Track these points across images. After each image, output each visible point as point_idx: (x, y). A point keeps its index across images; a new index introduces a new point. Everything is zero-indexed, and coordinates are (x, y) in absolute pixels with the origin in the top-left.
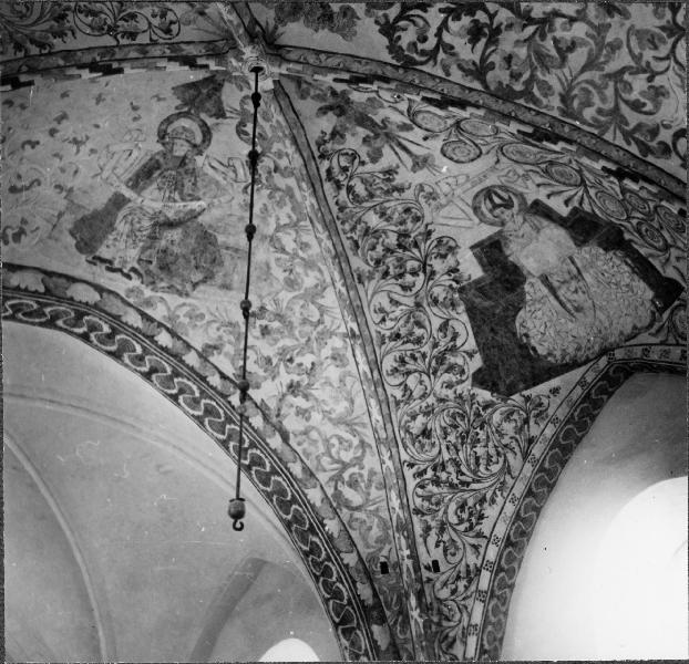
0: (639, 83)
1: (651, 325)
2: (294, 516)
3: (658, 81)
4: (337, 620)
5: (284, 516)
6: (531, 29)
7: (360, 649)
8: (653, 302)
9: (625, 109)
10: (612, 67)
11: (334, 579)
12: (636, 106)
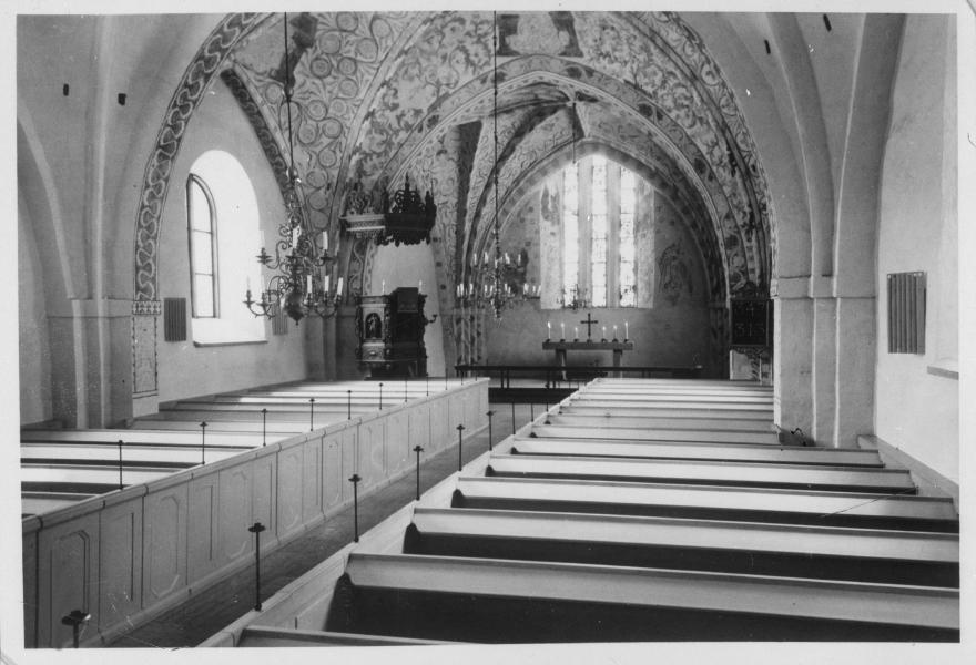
0: (415, 71)
1: (258, 74)
2: (210, 58)
3: (416, 79)
4: (162, 143)
5: (206, 51)
6: (439, 27)
7: (164, 174)
8: (272, 70)
9: (404, 68)
10: (421, 60)
11: (184, 117)
12: (406, 72)
